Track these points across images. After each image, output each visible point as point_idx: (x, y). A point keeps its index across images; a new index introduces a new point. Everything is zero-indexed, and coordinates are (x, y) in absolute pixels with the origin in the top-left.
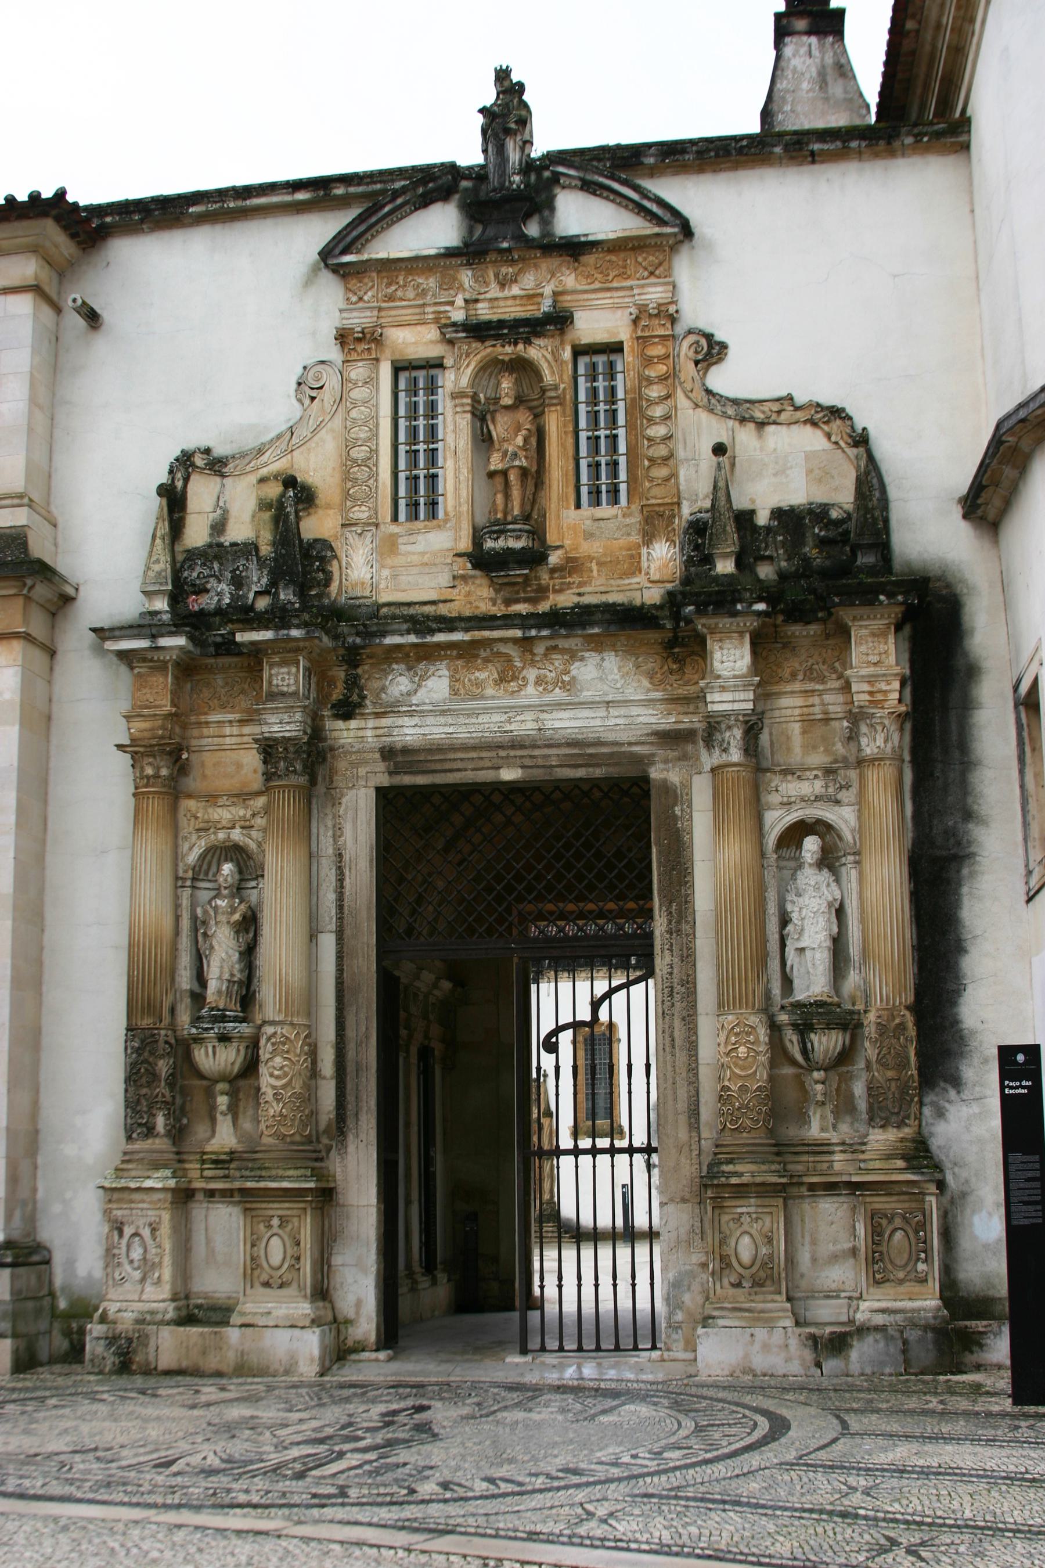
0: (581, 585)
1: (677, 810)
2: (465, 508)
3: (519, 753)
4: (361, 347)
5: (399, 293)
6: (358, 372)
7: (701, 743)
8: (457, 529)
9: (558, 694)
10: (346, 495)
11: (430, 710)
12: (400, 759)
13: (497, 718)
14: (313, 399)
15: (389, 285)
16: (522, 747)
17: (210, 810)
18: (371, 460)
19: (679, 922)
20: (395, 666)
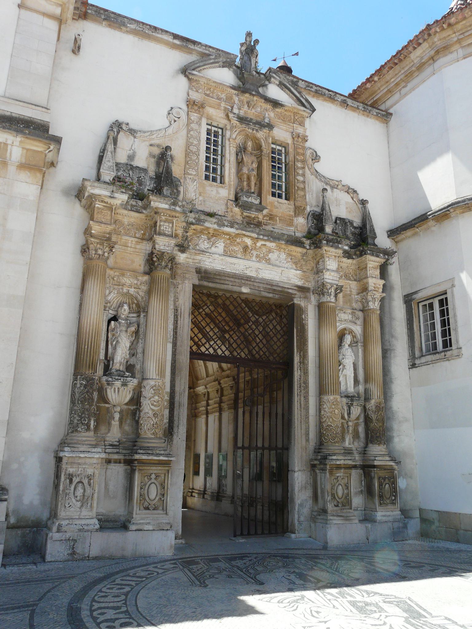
1: (303, 316)
2: (232, 183)
3: (249, 283)
6: (194, 116)
7: (311, 293)
8: (229, 191)
10: (187, 163)
11: (217, 257)
12: (203, 275)
14: (175, 121)
17: (121, 278)
19: (303, 359)
20: (202, 236)
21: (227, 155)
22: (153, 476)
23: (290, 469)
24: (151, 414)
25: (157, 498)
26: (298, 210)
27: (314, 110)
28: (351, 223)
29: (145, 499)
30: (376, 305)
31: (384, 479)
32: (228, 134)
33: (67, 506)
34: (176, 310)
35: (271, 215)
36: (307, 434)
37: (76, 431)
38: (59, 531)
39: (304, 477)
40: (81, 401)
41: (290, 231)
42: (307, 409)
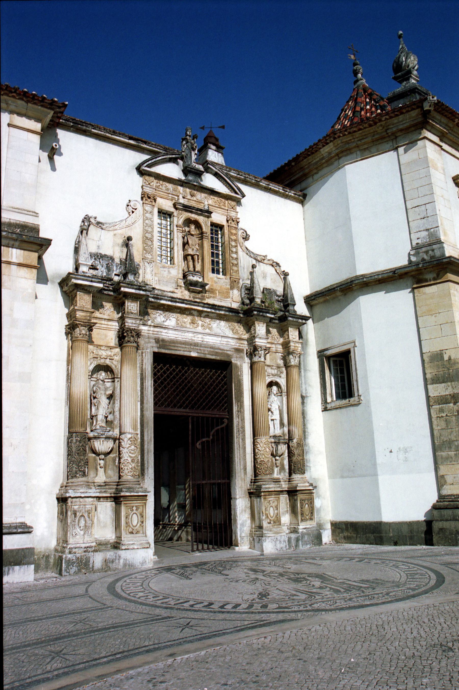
0: (214, 297)
4: (149, 200)
5: (161, 187)
6: (148, 208)
8: (178, 270)
9: (207, 331)
10: (144, 249)
13: (191, 335)
14: (133, 212)
15: (157, 183)
16: (197, 346)
17: (99, 350)
18: (151, 240)
21: (176, 239)
22: (134, 508)
23: (232, 496)
24: (130, 460)
25: (138, 525)
26: (234, 283)
27: (244, 196)
28: (275, 292)
29: (130, 526)
30: (296, 361)
31: (304, 500)
32: (175, 219)
33: (74, 534)
34: (142, 374)
35: (212, 289)
36: (245, 469)
37: (76, 476)
38: (70, 553)
39: (244, 502)
40: (78, 453)
41: (226, 303)
42: (244, 448)
